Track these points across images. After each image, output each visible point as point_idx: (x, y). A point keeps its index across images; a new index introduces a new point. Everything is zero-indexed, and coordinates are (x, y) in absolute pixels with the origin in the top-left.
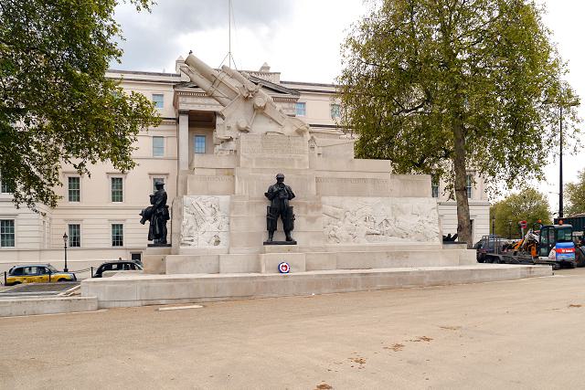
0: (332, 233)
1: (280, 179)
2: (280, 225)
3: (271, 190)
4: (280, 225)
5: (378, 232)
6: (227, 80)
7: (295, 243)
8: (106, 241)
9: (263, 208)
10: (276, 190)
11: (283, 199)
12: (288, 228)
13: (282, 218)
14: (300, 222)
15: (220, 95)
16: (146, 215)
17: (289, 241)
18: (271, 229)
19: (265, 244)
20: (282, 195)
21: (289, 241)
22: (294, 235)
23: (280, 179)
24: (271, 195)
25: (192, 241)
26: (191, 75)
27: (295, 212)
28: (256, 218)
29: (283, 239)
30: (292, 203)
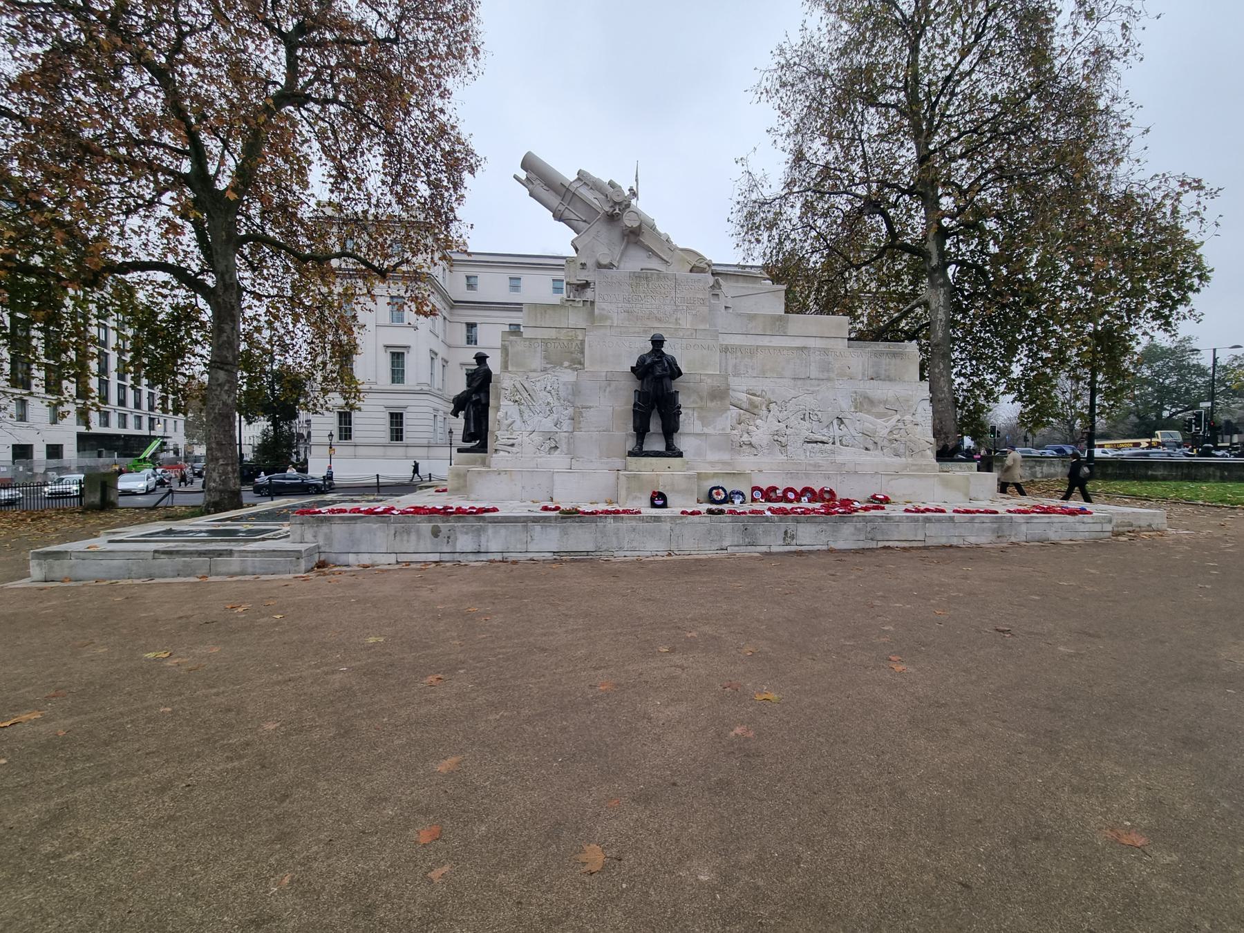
0: (745, 438)
1: (658, 343)
2: (655, 425)
3: (642, 360)
4: (655, 425)
5: (824, 439)
6: (585, 192)
7: (680, 455)
8: (383, 434)
9: (627, 389)
10: (649, 361)
11: (661, 378)
12: (670, 429)
13: (660, 411)
14: (689, 421)
15: (573, 217)
16: (460, 404)
17: (672, 451)
18: (641, 431)
19: (631, 454)
20: (658, 371)
21: (672, 451)
22: (682, 442)
23: (658, 343)
24: (642, 370)
25: (512, 445)
26: (531, 186)
27: (682, 400)
28: (612, 406)
29: (660, 446)
30: (677, 384)
